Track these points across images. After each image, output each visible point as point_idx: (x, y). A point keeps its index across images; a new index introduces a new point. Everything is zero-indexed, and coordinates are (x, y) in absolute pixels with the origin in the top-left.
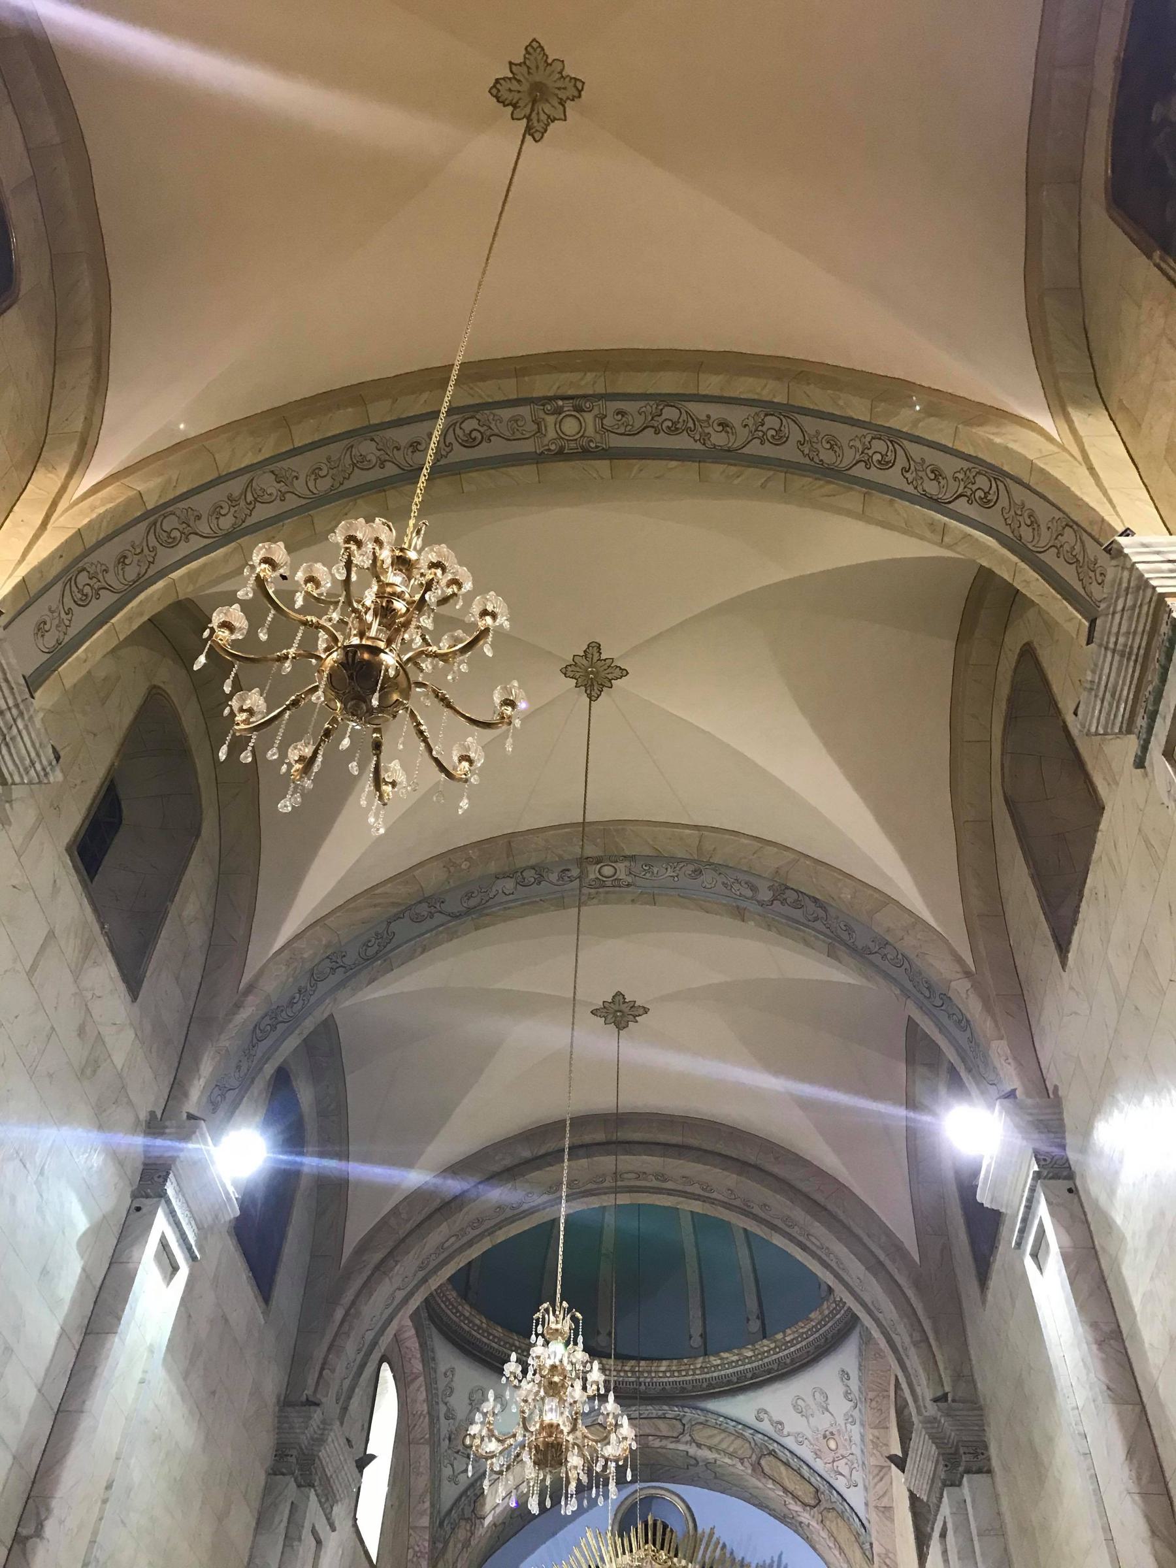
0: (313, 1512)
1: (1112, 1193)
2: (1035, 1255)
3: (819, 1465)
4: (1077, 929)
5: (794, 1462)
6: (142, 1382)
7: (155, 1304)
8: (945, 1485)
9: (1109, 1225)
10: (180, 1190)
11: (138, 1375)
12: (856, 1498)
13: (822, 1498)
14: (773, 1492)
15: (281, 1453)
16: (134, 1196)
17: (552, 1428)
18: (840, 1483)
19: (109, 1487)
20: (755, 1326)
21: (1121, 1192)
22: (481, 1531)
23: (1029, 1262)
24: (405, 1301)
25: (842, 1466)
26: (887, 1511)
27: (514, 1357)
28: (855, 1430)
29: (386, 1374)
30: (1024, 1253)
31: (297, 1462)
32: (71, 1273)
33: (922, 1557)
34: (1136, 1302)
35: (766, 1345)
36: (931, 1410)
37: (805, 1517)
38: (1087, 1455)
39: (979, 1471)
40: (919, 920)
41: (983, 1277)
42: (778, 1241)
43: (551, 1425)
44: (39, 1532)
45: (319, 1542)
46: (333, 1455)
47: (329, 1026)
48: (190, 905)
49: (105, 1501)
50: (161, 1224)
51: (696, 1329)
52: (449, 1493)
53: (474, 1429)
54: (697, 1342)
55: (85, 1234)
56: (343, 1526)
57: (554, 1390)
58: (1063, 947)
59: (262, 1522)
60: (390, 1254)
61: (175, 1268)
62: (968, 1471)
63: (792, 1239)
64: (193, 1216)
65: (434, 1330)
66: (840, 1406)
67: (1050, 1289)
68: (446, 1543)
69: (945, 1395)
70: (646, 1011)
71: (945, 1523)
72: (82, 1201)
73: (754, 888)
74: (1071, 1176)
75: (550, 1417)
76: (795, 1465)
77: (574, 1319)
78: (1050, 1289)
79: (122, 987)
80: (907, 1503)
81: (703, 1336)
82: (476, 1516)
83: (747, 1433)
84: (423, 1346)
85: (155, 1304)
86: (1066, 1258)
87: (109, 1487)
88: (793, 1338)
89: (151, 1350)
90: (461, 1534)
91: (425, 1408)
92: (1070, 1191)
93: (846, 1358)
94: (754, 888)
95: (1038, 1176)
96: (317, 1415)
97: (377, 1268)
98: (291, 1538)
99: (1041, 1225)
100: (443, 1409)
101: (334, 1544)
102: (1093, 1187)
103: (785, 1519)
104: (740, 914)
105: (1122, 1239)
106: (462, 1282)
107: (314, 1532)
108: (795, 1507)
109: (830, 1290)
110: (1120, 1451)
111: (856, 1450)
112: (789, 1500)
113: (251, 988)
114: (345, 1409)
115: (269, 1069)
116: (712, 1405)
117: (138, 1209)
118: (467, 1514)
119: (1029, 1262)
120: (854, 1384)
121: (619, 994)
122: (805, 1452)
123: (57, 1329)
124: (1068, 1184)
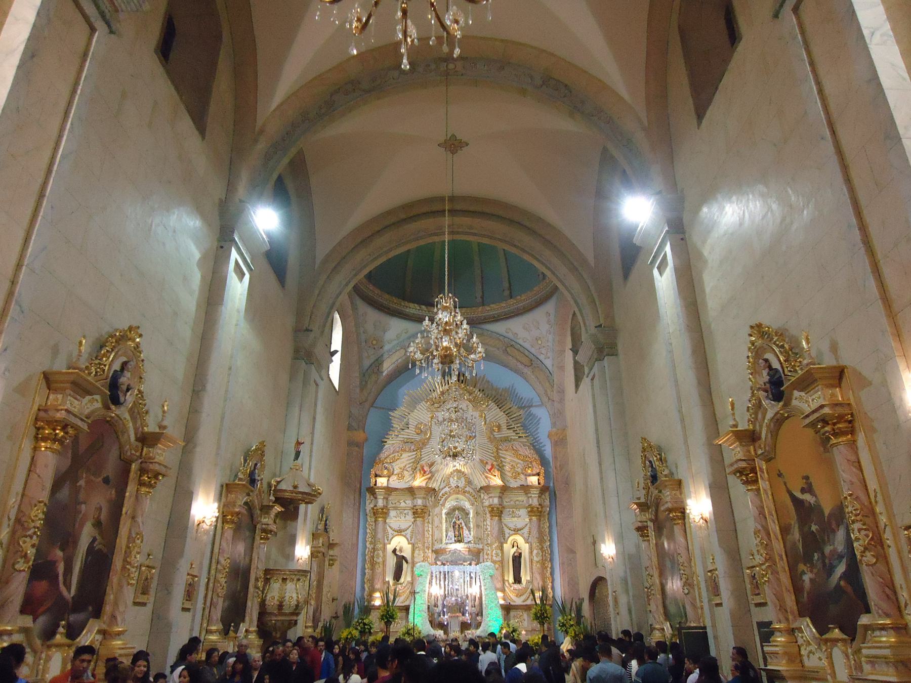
0: (314, 374)
1: (704, 242)
2: (659, 268)
3: (533, 350)
4: (710, 108)
5: (521, 349)
6: (236, 325)
7: (238, 289)
8: (596, 360)
9: (700, 255)
10: (241, 238)
11: (234, 322)
12: (548, 363)
13: (533, 362)
14: (512, 362)
15: (297, 351)
16: (219, 241)
17: (447, 349)
18: (542, 357)
19: (230, 369)
20: (507, 293)
21: (709, 241)
22: (382, 378)
23: (656, 272)
24: (347, 285)
25: (543, 351)
26: (562, 368)
27: (427, 318)
28: (550, 337)
29: (337, 316)
30: (653, 267)
31: (306, 353)
32: (196, 278)
33: (577, 386)
34: (708, 290)
35: (512, 301)
36: (593, 330)
37: (526, 370)
38: (671, 352)
39: (612, 355)
40: (621, 99)
41: (626, 276)
42: (526, 257)
43: (446, 347)
44: (204, 387)
45: (317, 385)
46: (319, 350)
47: (300, 153)
48: (223, 86)
49: (229, 375)
50: (234, 255)
51: (479, 294)
52: (367, 363)
53: (411, 349)
54: (479, 300)
55: (200, 260)
56: (325, 378)
57: (446, 332)
58: (700, 116)
59: (292, 377)
60: (338, 264)
61: (243, 274)
62: (608, 355)
63: (532, 256)
64: (248, 250)
65: (357, 298)
66: (545, 327)
67: (665, 283)
68: (366, 382)
69: (600, 326)
70: (467, 145)
71: (594, 376)
72: (195, 244)
73: (532, 77)
74: (684, 233)
75: (445, 344)
76: (522, 350)
77: (455, 302)
78: (665, 283)
79: (196, 133)
80: (572, 365)
81: (482, 297)
82: (379, 371)
83: (501, 338)
84: (352, 303)
85: (238, 289)
86: (677, 270)
87: (230, 369)
88: (523, 299)
89: (238, 311)
90: (374, 378)
91: (354, 329)
92: (682, 239)
93: (550, 306)
94: (532, 77)
95: (667, 232)
96: (312, 335)
97: (333, 270)
98: (305, 383)
99: (665, 255)
100: (362, 330)
101: (323, 385)
102: (695, 238)
103: (516, 371)
104: (523, 92)
105: (706, 262)
106: (369, 277)
107: (315, 381)
108: (521, 366)
109: (544, 276)
110: (689, 351)
111: (550, 344)
112: (519, 364)
113: (262, 131)
114: (323, 332)
115: (275, 176)
116: (483, 326)
117: (222, 247)
118: (375, 370)
119: (656, 272)
120: (552, 317)
121: (453, 135)
122: (527, 345)
123: (195, 303)
124: (681, 236)
